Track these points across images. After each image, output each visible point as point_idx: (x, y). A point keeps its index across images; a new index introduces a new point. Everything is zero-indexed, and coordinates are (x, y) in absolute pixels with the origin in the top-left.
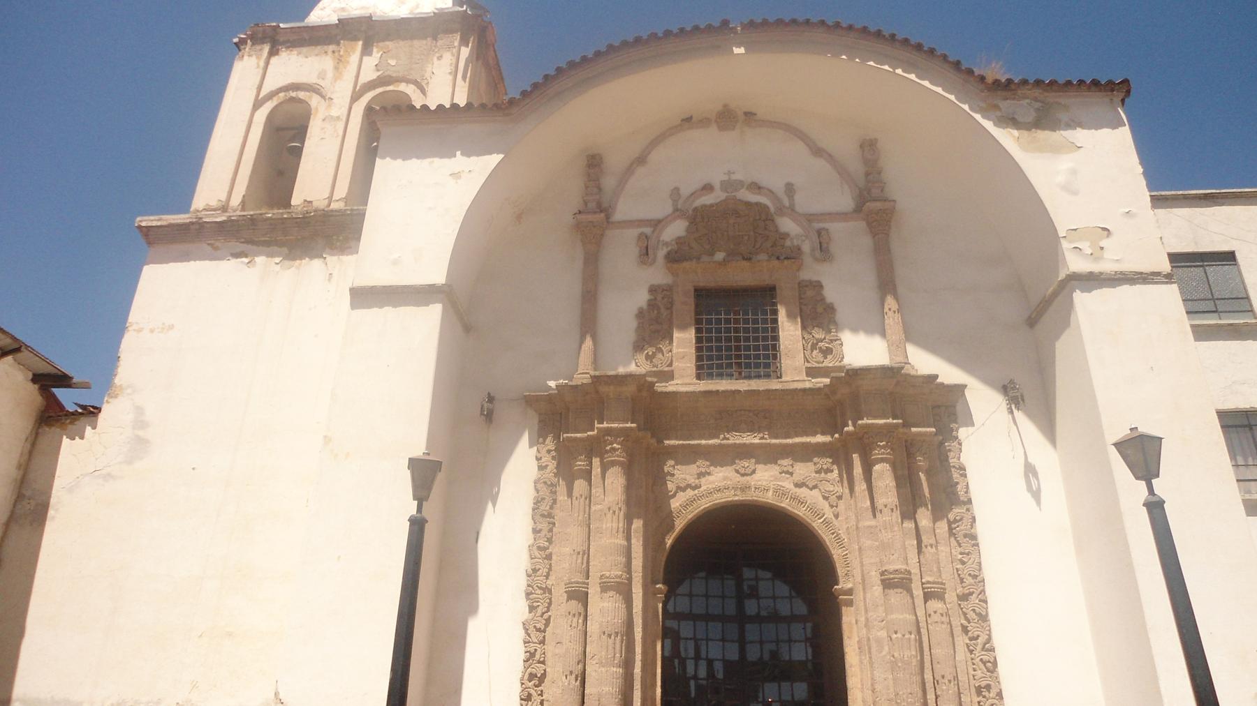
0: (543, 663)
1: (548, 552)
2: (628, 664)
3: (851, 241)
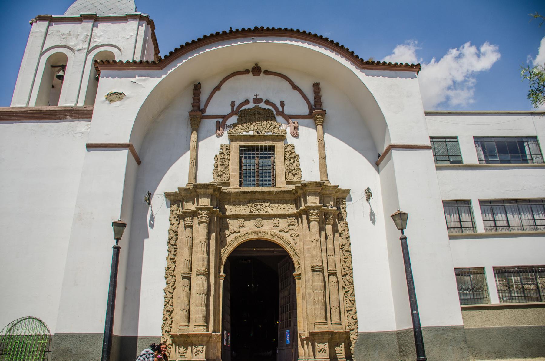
0: (172, 306)
1: (174, 260)
2: (207, 306)
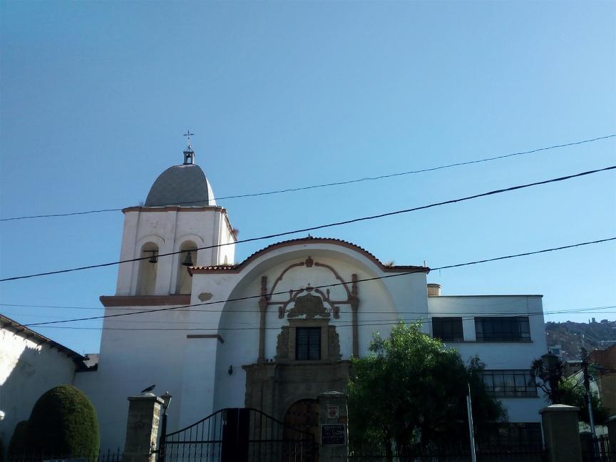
3: (346, 309)
